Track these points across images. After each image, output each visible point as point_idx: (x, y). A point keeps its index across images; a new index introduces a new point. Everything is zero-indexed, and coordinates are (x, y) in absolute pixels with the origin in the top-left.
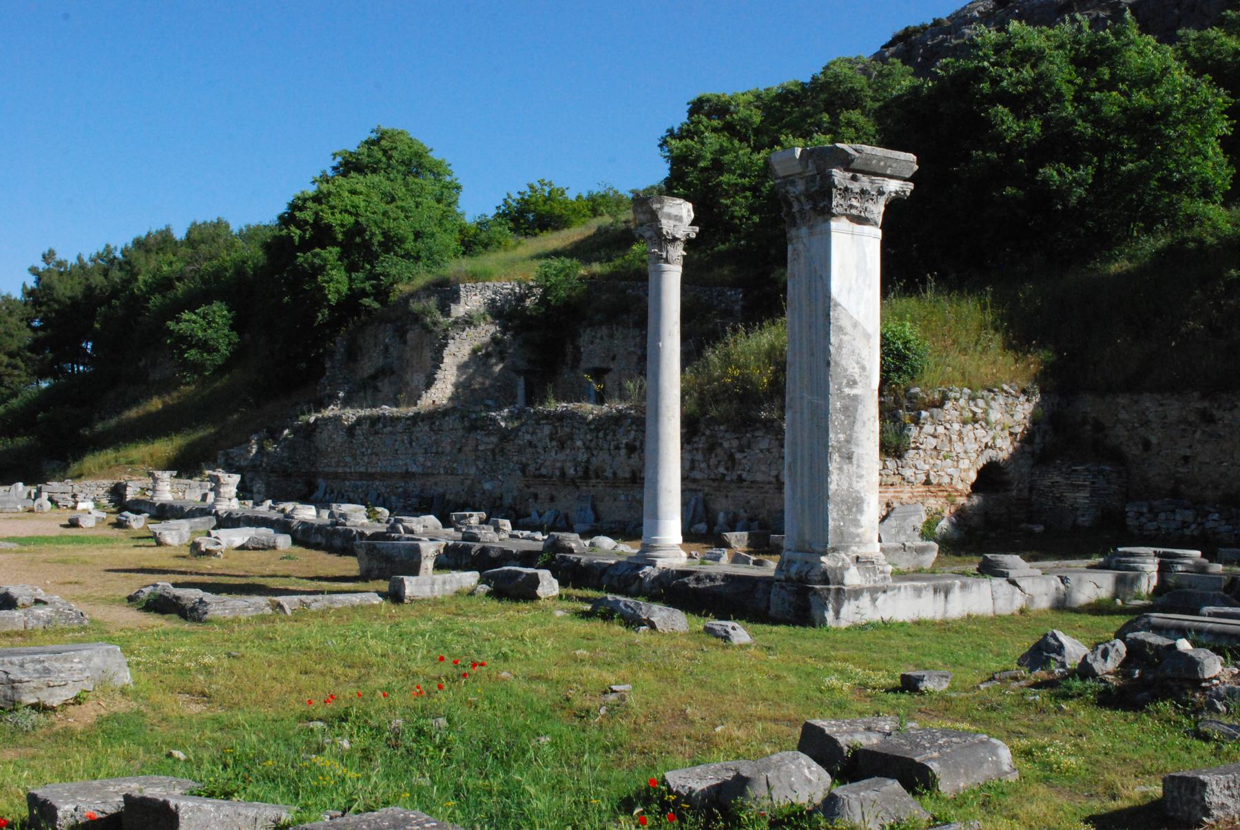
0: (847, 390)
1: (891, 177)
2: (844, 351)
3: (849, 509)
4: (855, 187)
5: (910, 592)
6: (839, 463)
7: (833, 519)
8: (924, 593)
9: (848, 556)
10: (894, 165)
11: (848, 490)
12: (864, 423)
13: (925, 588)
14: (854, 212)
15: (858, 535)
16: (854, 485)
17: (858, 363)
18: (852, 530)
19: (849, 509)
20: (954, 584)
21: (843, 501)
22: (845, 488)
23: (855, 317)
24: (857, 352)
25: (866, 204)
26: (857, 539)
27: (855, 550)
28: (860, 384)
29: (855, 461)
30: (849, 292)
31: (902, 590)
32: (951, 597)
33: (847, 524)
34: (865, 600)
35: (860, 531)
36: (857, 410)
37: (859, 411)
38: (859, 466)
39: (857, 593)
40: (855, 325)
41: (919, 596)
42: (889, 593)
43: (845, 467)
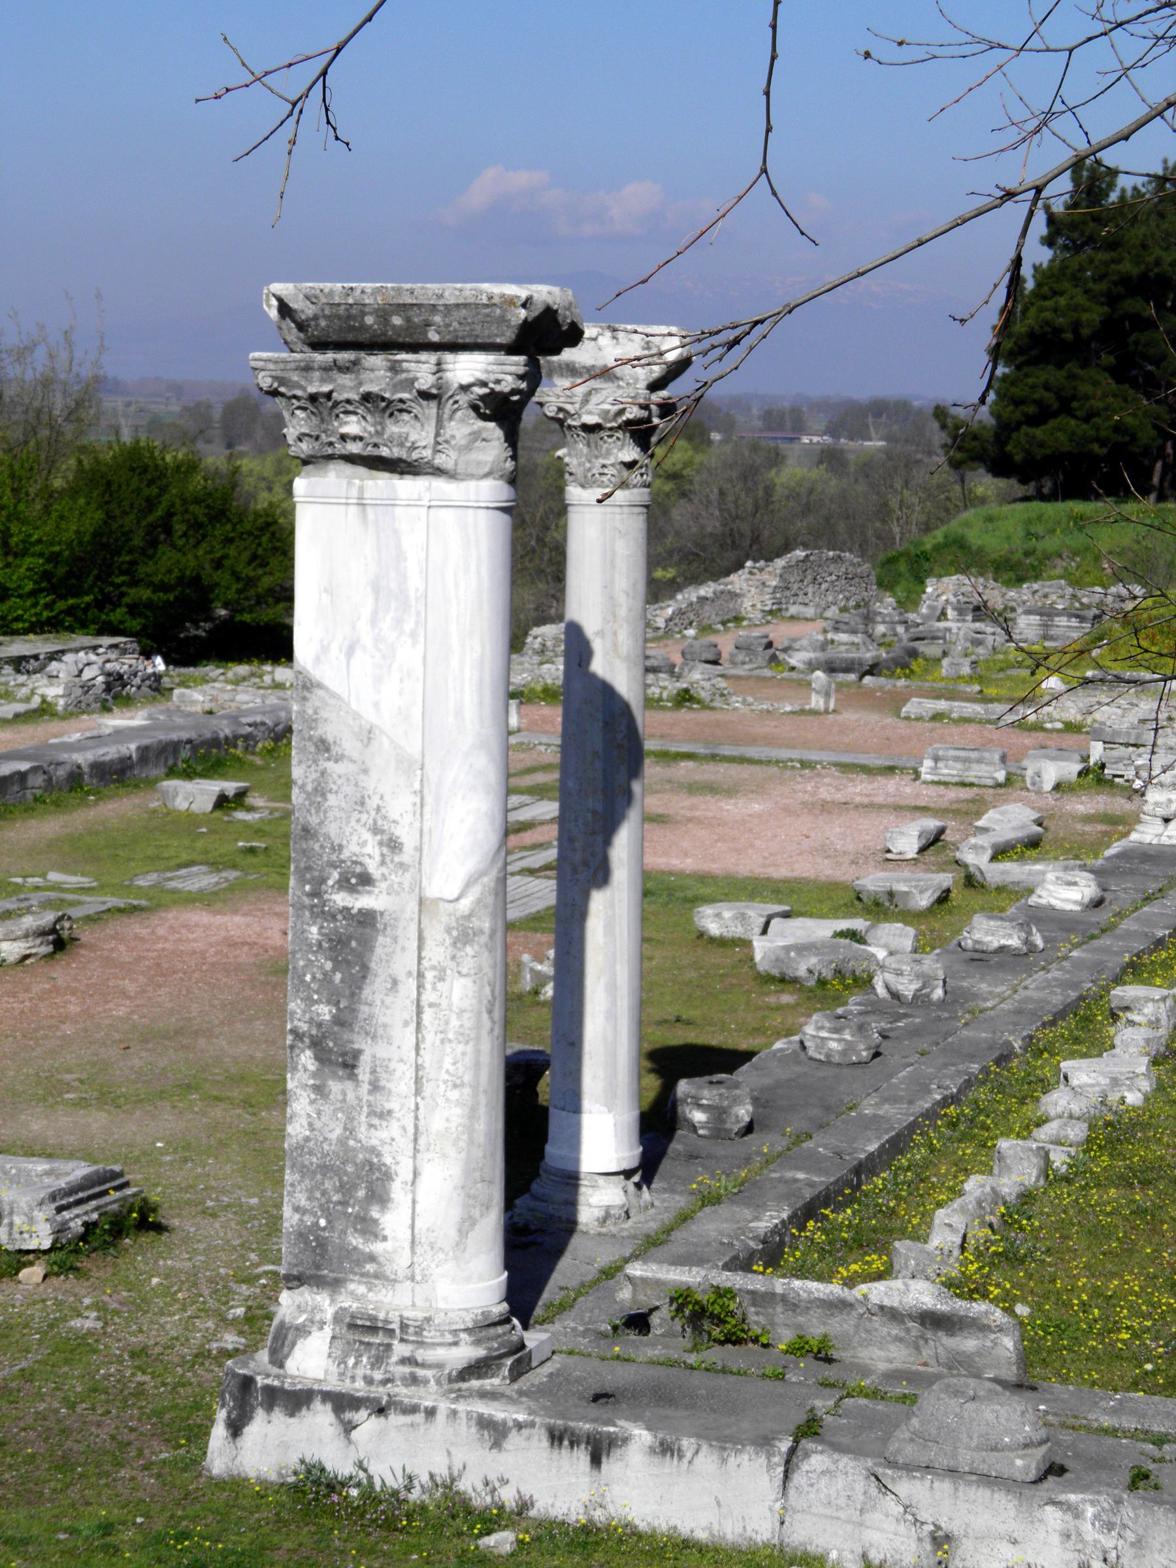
0: (341, 899)
1: (455, 347)
2: (332, 800)
3: (347, 1189)
4: (346, 387)
5: (466, 1431)
6: (314, 1075)
7: (297, 1209)
8: (514, 1440)
9: (333, 1301)
10: (437, 319)
11: (342, 1142)
12: (395, 982)
13: (520, 1426)
14: (354, 448)
15: (372, 1258)
16: (362, 1132)
17: (376, 830)
18: (356, 1240)
19: (347, 1189)
20: (626, 1440)
21: (325, 1169)
22: (334, 1136)
23: (370, 716)
25: (393, 429)
26: (370, 1267)
28: (383, 885)
29: (363, 1072)
30: (350, 651)
31: (441, 1417)
33: (339, 1225)
34: (321, 1417)
35: (377, 1247)
36: (371, 949)
37: (379, 952)
38: (375, 1087)
40: (368, 736)
41: (497, 1445)
42: (395, 1419)
43: (335, 1087)
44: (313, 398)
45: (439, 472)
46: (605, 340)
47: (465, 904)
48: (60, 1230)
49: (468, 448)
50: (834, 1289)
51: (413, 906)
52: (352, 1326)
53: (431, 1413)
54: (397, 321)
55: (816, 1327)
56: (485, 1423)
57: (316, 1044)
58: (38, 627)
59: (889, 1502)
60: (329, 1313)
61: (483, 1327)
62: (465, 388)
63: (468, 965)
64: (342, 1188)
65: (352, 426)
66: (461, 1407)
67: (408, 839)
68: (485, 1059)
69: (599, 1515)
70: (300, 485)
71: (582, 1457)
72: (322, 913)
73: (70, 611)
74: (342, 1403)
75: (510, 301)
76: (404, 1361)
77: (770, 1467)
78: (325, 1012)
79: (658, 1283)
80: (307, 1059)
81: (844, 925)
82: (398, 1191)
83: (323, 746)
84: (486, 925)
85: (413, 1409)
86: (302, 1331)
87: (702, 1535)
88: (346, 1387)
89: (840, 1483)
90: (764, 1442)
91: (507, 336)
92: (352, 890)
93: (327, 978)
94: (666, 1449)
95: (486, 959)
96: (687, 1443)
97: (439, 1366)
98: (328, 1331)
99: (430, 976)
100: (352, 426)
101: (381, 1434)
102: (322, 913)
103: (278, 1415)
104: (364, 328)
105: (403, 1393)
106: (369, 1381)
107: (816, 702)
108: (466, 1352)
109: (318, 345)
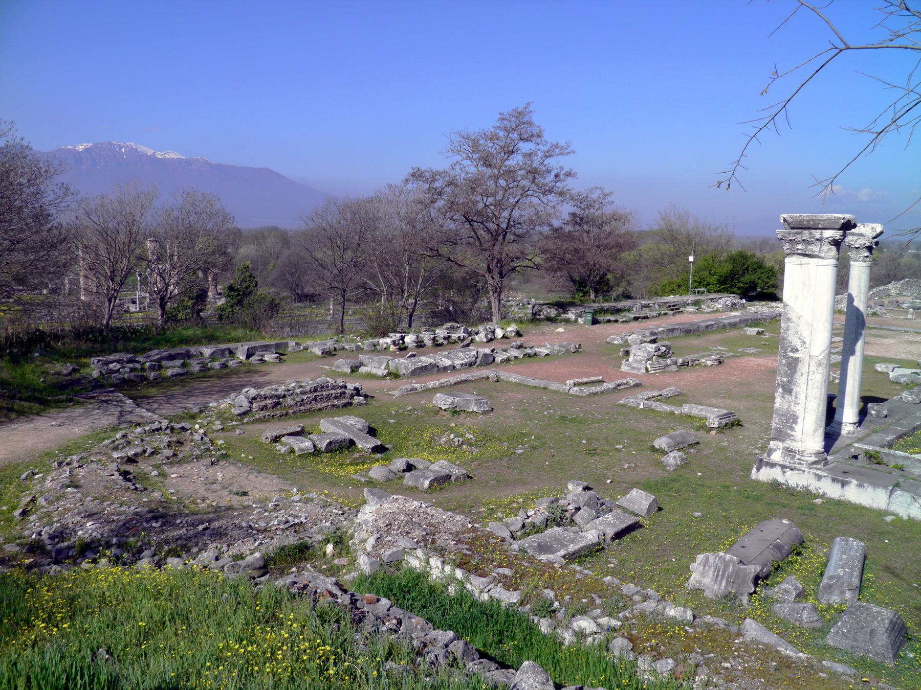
0: (791, 354)
2: (790, 332)
3: (788, 420)
4: (799, 238)
5: (812, 476)
8: (823, 479)
11: (787, 409)
13: (825, 476)
14: (800, 252)
15: (792, 436)
16: (792, 407)
17: (800, 339)
18: (789, 431)
19: (788, 420)
21: (783, 415)
24: (799, 333)
25: (809, 247)
27: (788, 444)
29: (793, 394)
31: (806, 472)
32: (846, 488)
34: (778, 470)
35: (794, 433)
38: (796, 397)
39: (772, 465)
40: (799, 317)
42: (795, 472)
43: (786, 396)
44: (791, 240)
45: (820, 257)
46: (862, 227)
47: (820, 358)
48: (720, 424)
49: (827, 252)
50: (907, 454)
51: (808, 357)
52: (787, 450)
53: (804, 471)
54: (812, 223)
55: (901, 463)
56: (816, 475)
57: (783, 387)
58: (716, 292)
59: (917, 504)
60: (781, 447)
61: (818, 454)
62: (827, 238)
63: (820, 371)
64: (786, 419)
65: (800, 247)
66: (811, 471)
67: (808, 341)
68: (823, 393)
69: (842, 498)
70: (787, 260)
71: (839, 485)
72: (786, 357)
73: (724, 288)
74: (783, 467)
75: (840, 218)
76: (798, 459)
77: (886, 492)
78: (785, 379)
79: (861, 448)
80: (780, 390)
81: (914, 371)
82: (800, 421)
83: (789, 319)
84: (825, 362)
85: (800, 470)
86: (775, 450)
87: (868, 506)
88: (784, 463)
89: (904, 498)
90: (885, 487)
91: (839, 226)
92: (794, 352)
93: (786, 372)
94: (860, 485)
95: (825, 370)
96: (865, 485)
97: (807, 461)
98: (781, 451)
99: (811, 373)
100: (800, 247)
101: (792, 475)
102: (786, 357)
103: (768, 468)
104: (804, 224)
105: (798, 466)
106: (790, 463)
107: (910, 316)
108: (813, 459)
109: (793, 228)
